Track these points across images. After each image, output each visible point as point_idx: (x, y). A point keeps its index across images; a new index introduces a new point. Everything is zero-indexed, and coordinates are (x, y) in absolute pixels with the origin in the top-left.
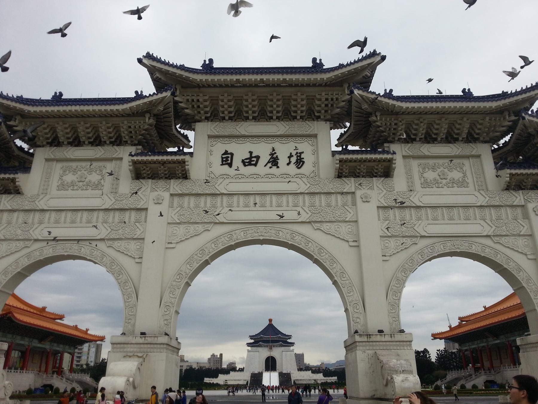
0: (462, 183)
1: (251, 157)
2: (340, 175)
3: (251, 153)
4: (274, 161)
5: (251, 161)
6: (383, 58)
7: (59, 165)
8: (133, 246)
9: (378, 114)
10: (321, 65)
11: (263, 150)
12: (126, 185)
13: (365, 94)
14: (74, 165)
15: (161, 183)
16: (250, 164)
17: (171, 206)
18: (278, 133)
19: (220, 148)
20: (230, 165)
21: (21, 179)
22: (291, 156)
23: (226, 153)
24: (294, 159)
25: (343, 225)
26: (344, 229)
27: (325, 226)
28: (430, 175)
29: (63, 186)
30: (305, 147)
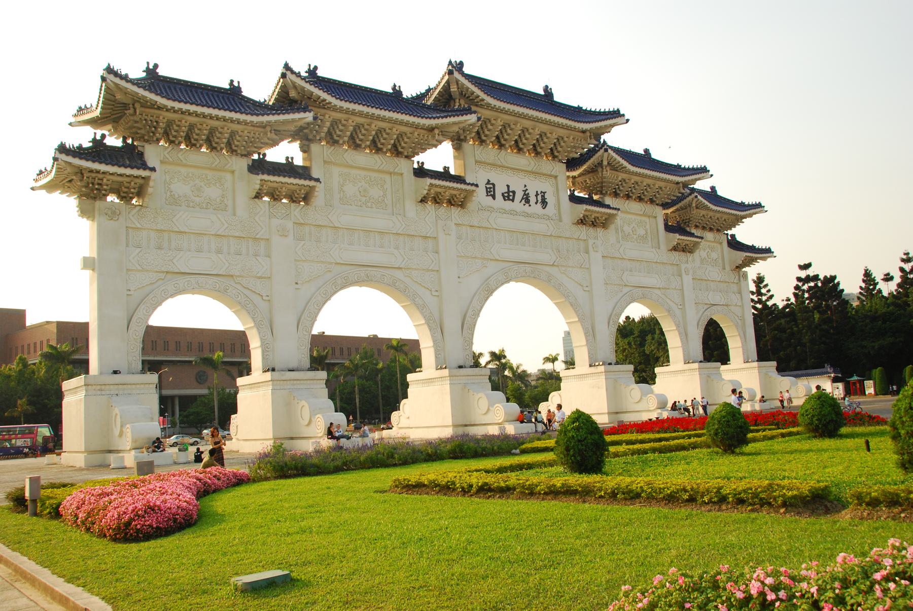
1: (508, 192)
3: (508, 186)
5: (509, 196)
6: (628, 121)
7: (336, 171)
9: (608, 168)
12: (411, 208)
14: (354, 172)
15: (444, 209)
16: (509, 199)
18: (530, 169)
20: (494, 197)
22: (537, 195)
24: (539, 198)
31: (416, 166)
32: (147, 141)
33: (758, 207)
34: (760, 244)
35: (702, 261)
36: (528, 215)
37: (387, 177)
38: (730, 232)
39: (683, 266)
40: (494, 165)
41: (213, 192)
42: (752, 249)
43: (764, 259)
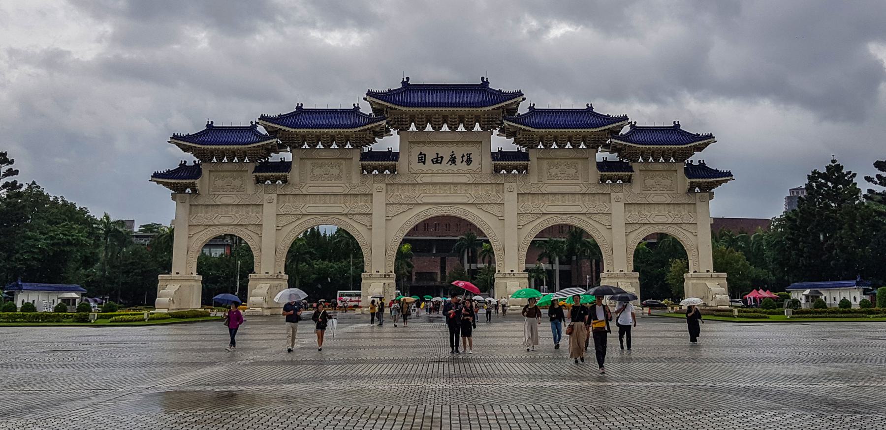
0: (575, 178)
2: (497, 170)
4: (453, 160)
5: (438, 160)
6: (524, 99)
7: (309, 162)
8: (365, 220)
10: (487, 82)
11: (445, 152)
12: (356, 179)
13: (511, 123)
17: (387, 192)
19: (416, 150)
20: (424, 163)
21: (289, 175)
23: (421, 154)
24: (465, 159)
25: (496, 206)
26: (495, 209)
27: (484, 207)
28: (554, 171)
29: (314, 178)
30: (473, 150)
31: (366, 149)
32: (205, 161)
33: (711, 136)
34: (722, 169)
35: (646, 188)
36: (453, 173)
37: (343, 162)
38: (696, 158)
39: (613, 195)
40: (424, 142)
41: (237, 182)
42: (716, 173)
43: (726, 181)
